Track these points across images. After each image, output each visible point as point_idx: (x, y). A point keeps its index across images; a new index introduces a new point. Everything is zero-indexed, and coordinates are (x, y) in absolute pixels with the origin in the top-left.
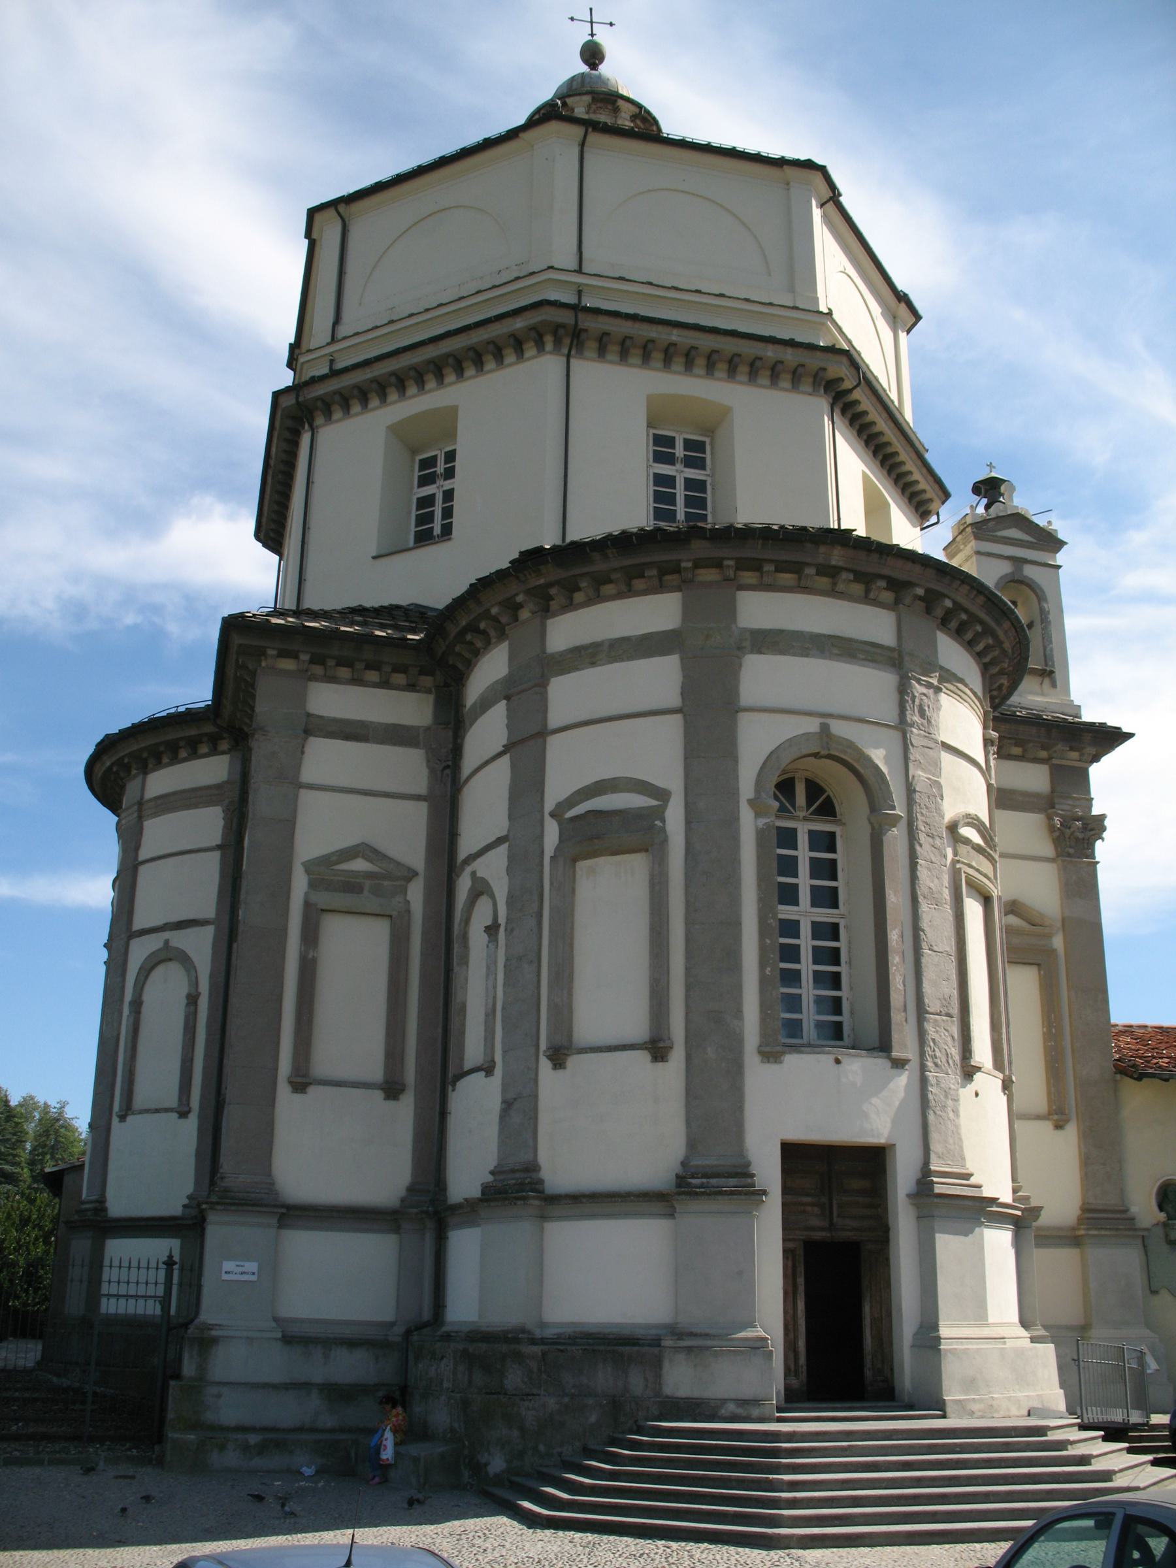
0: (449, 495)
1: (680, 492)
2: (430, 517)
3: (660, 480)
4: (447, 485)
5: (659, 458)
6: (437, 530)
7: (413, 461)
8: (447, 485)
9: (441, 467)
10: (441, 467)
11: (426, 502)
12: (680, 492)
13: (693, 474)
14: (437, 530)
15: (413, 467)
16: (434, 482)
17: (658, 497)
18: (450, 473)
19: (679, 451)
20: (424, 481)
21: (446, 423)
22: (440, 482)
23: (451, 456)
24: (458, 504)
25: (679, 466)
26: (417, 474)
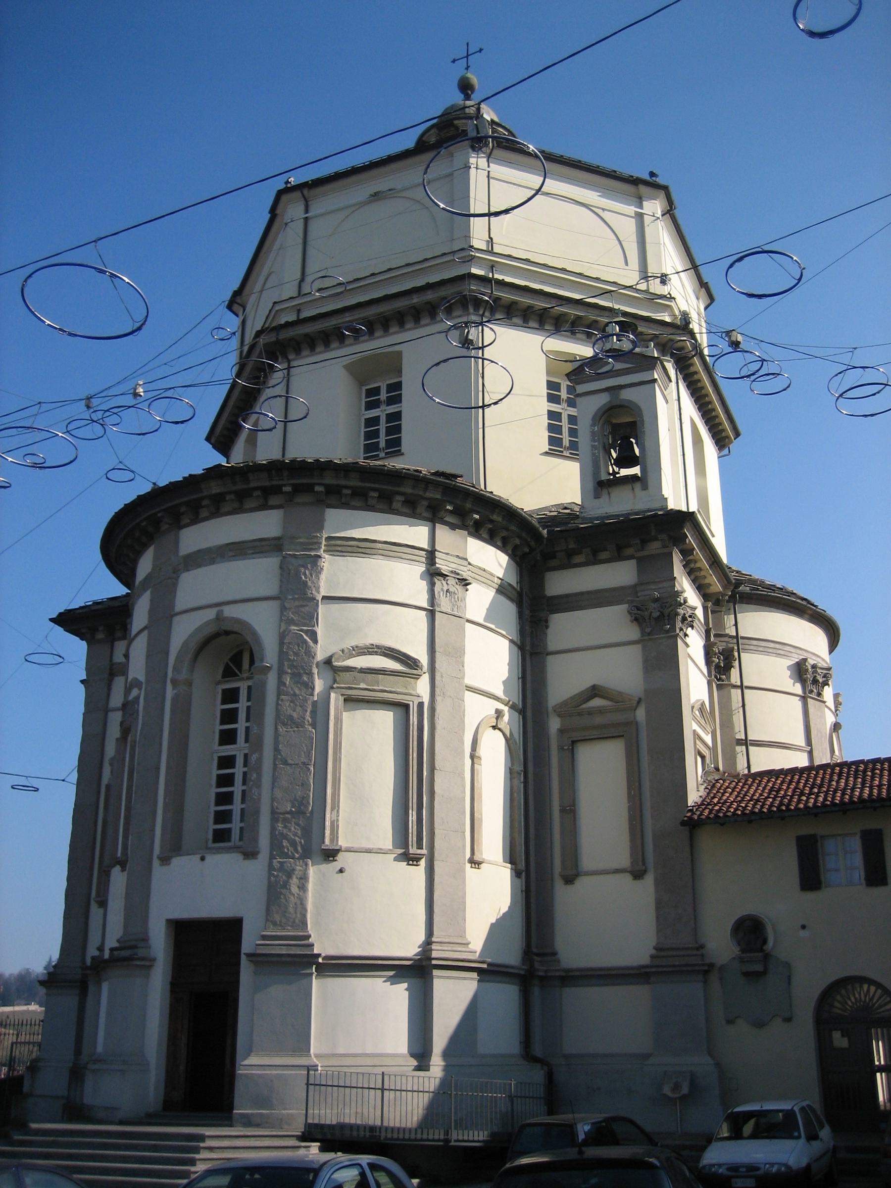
0: (396, 417)
1: (565, 424)
2: (376, 434)
3: (552, 415)
4: (392, 409)
5: (553, 398)
6: (382, 444)
7: (361, 389)
8: (392, 409)
9: (383, 396)
10: (383, 396)
11: (372, 422)
12: (565, 424)
13: (573, 411)
14: (382, 444)
15: (360, 394)
16: (379, 407)
17: (551, 428)
18: (397, 399)
19: (564, 394)
20: (370, 406)
21: (393, 363)
22: (383, 407)
23: (398, 386)
24: (406, 423)
25: (565, 405)
26: (364, 400)
